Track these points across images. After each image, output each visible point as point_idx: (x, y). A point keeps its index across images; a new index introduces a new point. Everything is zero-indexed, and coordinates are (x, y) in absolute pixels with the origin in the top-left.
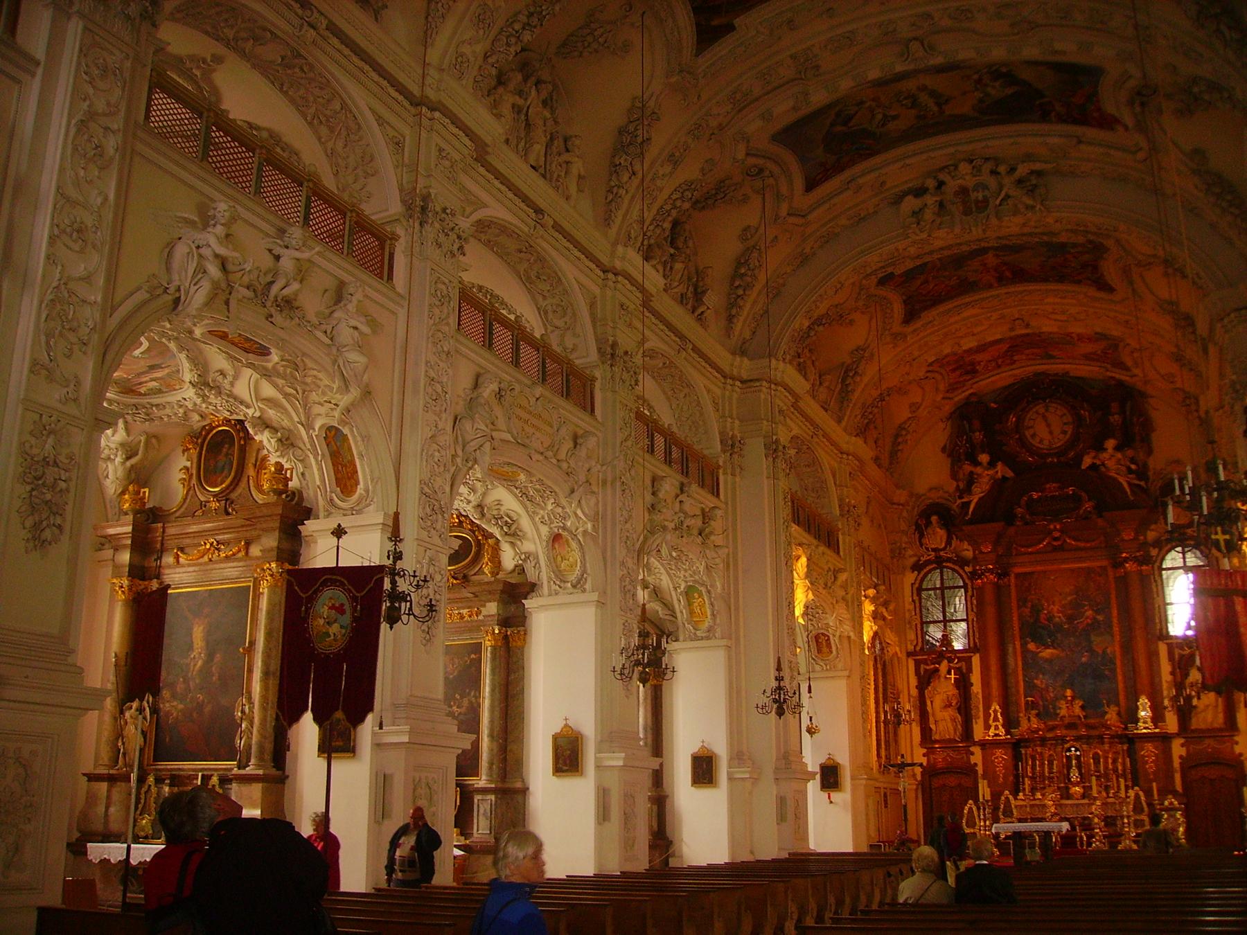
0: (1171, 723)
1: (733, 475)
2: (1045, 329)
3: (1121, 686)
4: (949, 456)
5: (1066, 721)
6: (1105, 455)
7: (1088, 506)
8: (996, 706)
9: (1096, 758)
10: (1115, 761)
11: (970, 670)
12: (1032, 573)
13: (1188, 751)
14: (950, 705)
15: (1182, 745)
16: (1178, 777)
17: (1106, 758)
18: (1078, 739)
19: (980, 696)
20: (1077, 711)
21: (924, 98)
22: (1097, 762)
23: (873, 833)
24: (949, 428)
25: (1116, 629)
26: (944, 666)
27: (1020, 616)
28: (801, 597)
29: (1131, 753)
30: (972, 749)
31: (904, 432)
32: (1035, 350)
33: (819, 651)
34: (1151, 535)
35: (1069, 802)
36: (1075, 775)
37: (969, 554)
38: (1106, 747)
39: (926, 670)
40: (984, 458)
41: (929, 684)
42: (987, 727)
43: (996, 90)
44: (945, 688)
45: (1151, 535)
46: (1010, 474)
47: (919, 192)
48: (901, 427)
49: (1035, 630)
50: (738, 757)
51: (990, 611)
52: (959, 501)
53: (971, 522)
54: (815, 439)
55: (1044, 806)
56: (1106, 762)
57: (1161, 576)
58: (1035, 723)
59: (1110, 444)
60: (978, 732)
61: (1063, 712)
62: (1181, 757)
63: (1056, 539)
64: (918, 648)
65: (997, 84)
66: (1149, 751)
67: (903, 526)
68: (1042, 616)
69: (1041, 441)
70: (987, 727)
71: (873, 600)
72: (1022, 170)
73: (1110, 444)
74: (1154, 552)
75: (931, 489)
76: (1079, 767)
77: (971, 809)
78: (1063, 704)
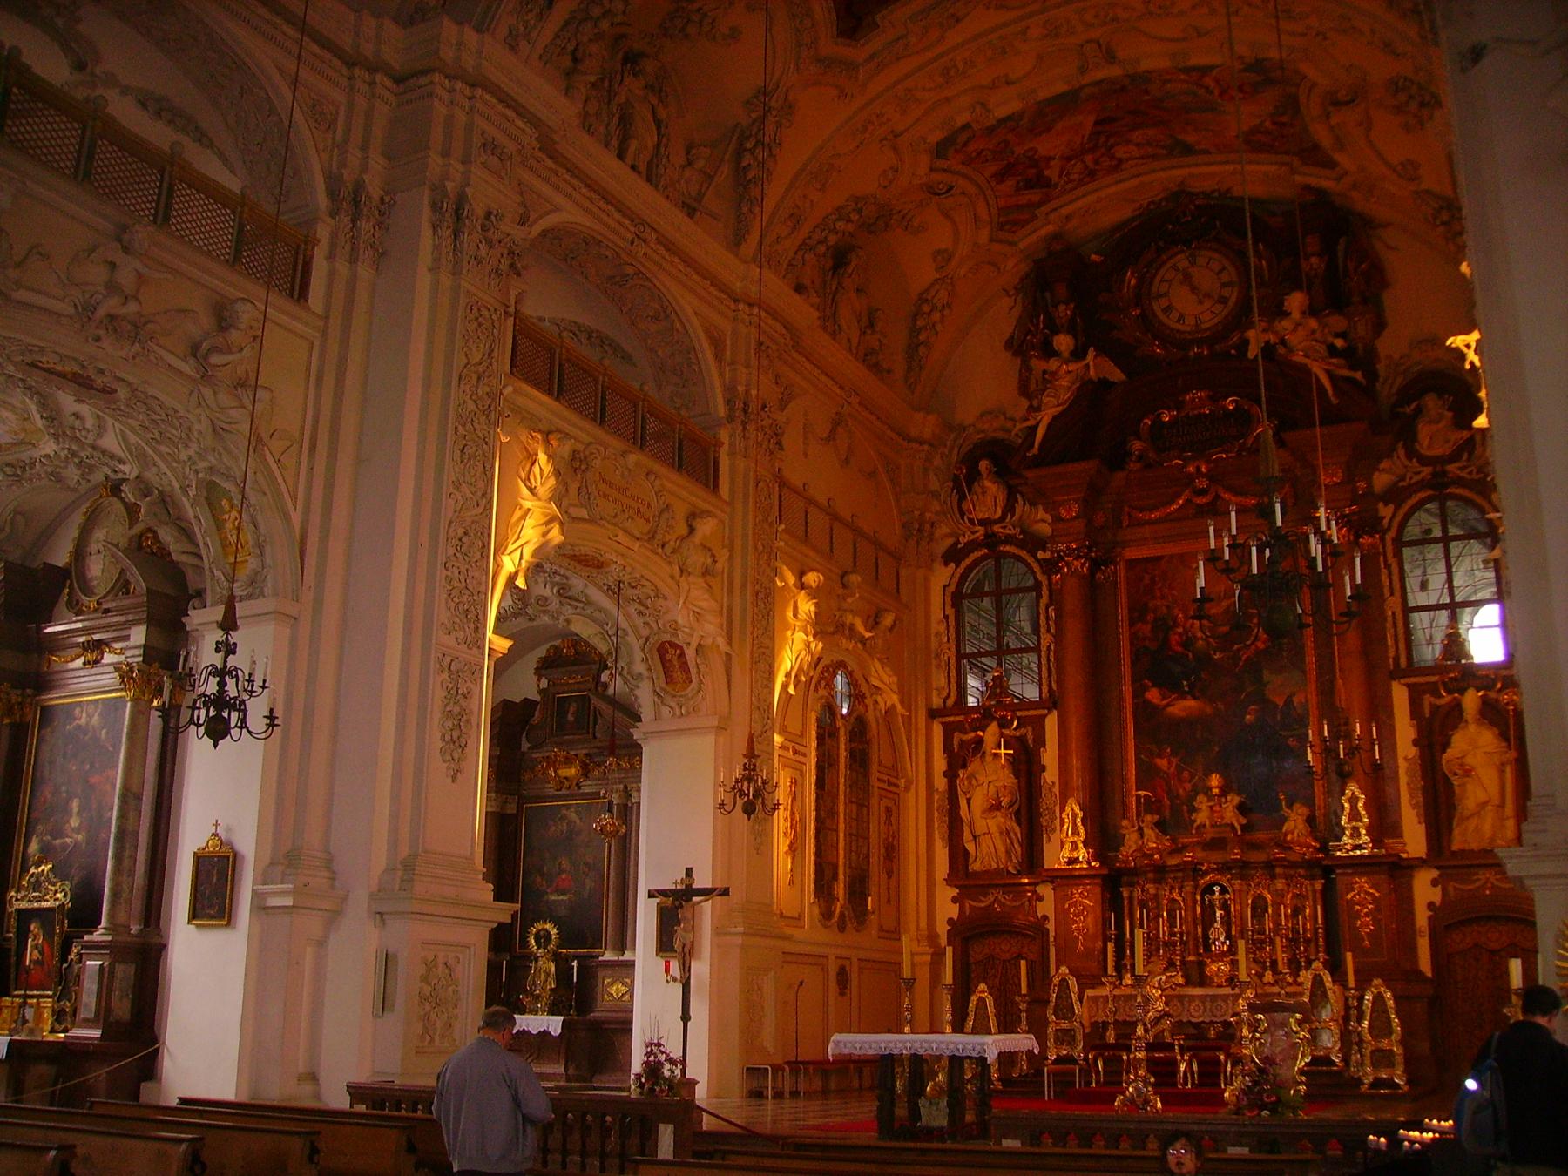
0: (1414, 841)
1: (353, 260)
2: (1146, 65)
4: (1015, 354)
5: (1209, 834)
6: (1286, 324)
11: (1041, 741)
12: (1162, 557)
13: (1444, 891)
15: (1434, 883)
16: (1424, 946)
18: (1224, 868)
19: (1056, 790)
20: (1230, 814)
23: (768, 1038)
24: (1018, 308)
25: (1310, 659)
26: (991, 734)
27: (1133, 638)
29: (1329, 897)
30: (1041, 889)
31: (926, 308)
32: (1151, 132)
33: (669, 679)
34: (1381, 480)
35: (1198, 991)
36: (1218, 933)
38: (1280, 884)
39: (962, 742)
44: (992, 776)
45: (1381, 480)
46: (1117, 375)
48: (922, 299)
49: (1162, 665)
50: (286, 859)
51: (1074, 631)
53: (1038, 462)
54: (641, 250)
57: (1398, 555)
58: (1152, 839)
59: (1295, 301)
61: (1202, 817)
62: (1431, 905)
63: (1202, 492)
64: (951, 702)
66: (1361, 892)
67: (934, 484)
68: (1174, 638)
69: (1181, 317)
71: (813, 594)
73: (1295, 301)
74: (1386, 511)
75: (982, 415)
76: (1227, 923)
78: (1202, 802)
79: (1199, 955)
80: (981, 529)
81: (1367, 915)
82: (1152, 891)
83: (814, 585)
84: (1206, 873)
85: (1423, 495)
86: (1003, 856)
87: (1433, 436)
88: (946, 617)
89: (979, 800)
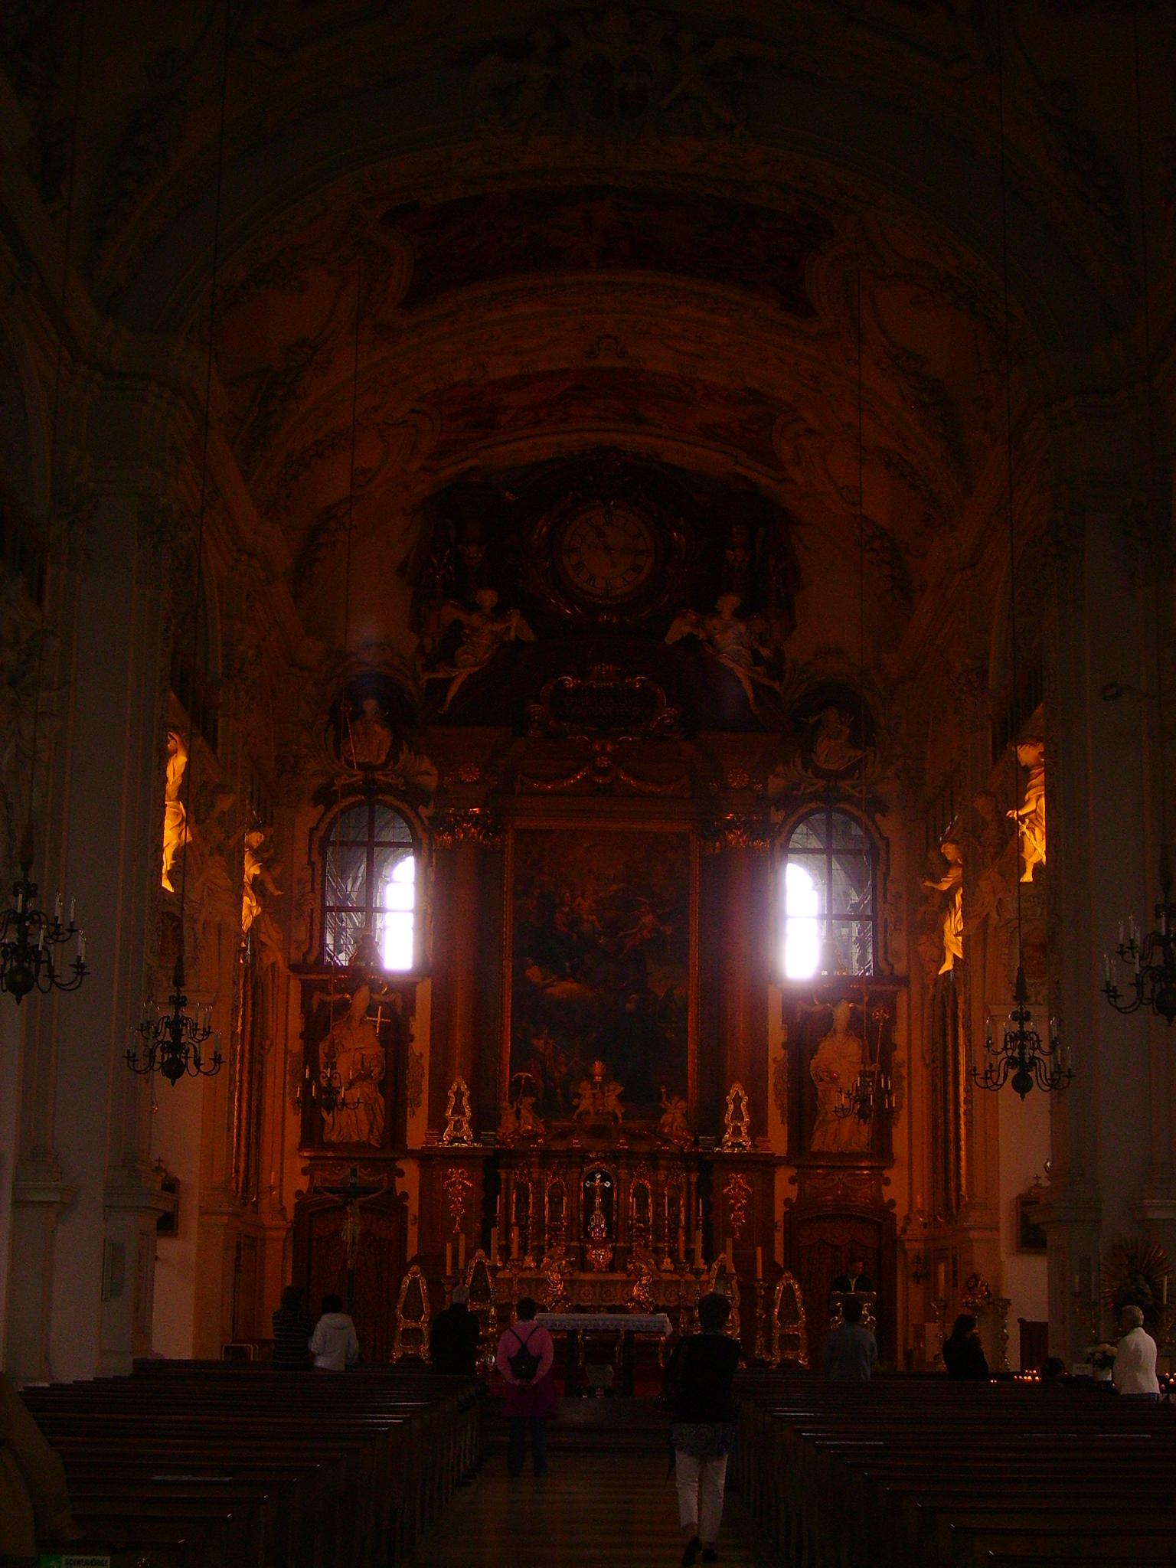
0: (777, 1140)
3: (692, 1062)
8: (460, 1084)
9: (641, 1195)
10: (673, 1202)
13: (800, 1189)
14: (368, 1075)
15: (792, 1181)
16: (779, 1237)
17: (658, 1198)
19: (426, 1061)
20: (612, 1103)
22: (642, 1205)
28: (171, 837)
30: (401, 1165)
35: (588, 1277)
36: (598, 1225)
37: (431, 782)
40: (488, 598)
41: (327, 1029)
42: (437, 1123)
45: (775, 785)
52: (426, 676)
55: (545, 1282)
56: (658, 1205)
59: (729, 603)
60: (417, 1132)
61: (586, 1104)
62: (787, 1201)
64: (312, 958)
66: (736, 1186)
70: (437, 1123)
73: (729, 603)
76: (607, 1209)
77: (414, 1281)
79: (579, 1240)
80: (360, 774)
81: (740, 1209)
82: (535, 1175)
83: (255, 845)
84: (592, 1161)
85: (813, 806)
86: (366, 1129)
88: (311, 864)
89: (345, 1067)
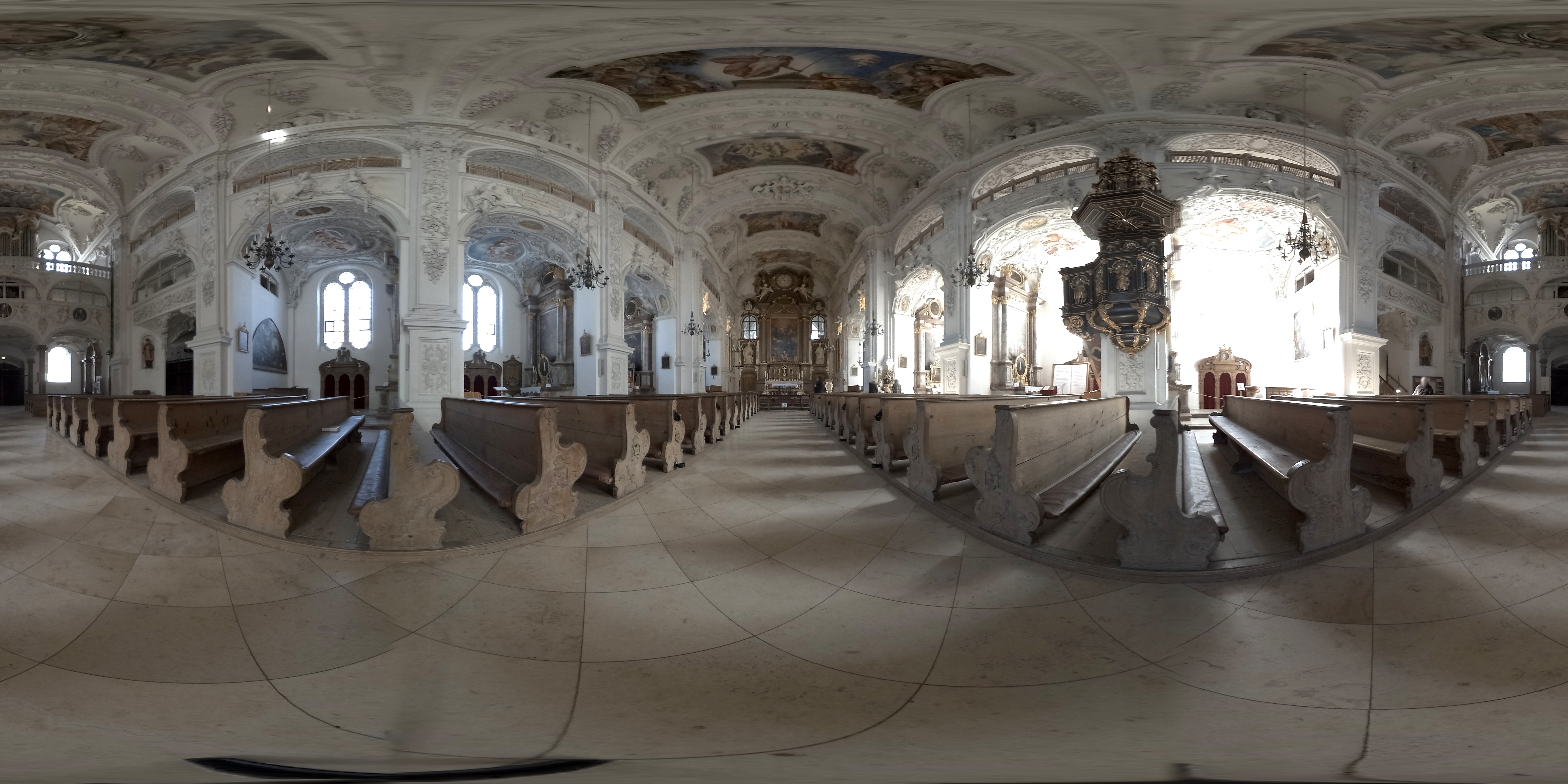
7: (794, 302)
21: (776, 148)
43: (812, 151)
47: (763, 185)
59: (803, 285)
65: (813, 149)
72: (806, 185)
73: (803, 285)
87: (819, 307)
